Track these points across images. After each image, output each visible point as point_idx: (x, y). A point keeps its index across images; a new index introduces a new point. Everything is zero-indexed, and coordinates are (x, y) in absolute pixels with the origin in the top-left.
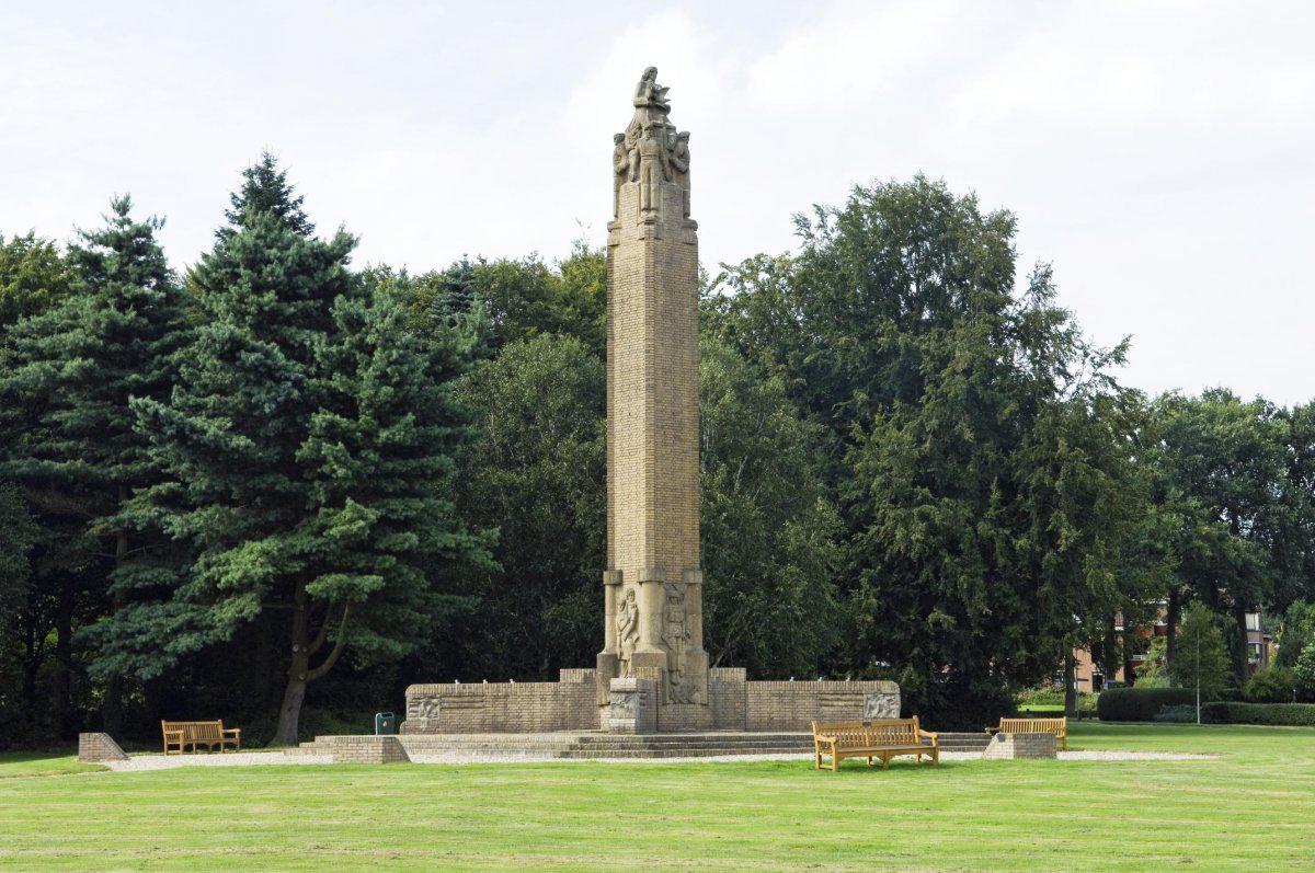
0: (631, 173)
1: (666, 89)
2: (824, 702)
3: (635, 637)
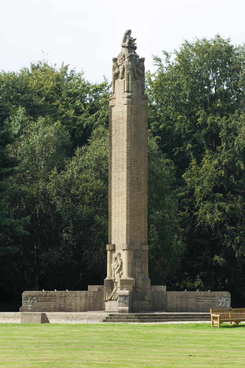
0: (120, 75)
1: (135, 39)
2: (199, 300)
3: (121, 273)
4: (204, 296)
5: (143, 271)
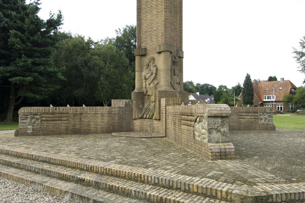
3: (156, 82)
4: (246, 112)
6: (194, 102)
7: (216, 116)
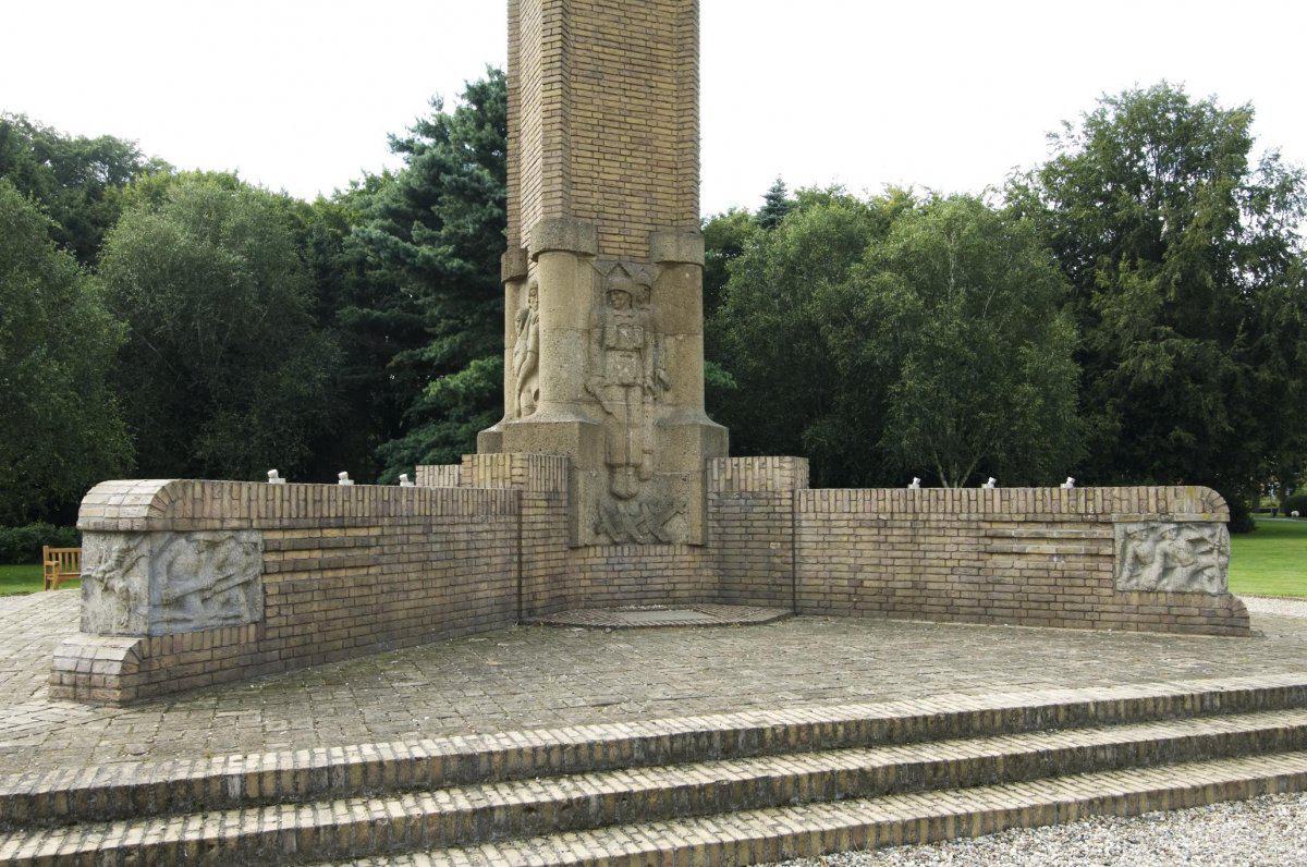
2: (997, 544)
4: (1030, 517)
5: (662, 374)
6: (733, 469)
7: (101, 527)
